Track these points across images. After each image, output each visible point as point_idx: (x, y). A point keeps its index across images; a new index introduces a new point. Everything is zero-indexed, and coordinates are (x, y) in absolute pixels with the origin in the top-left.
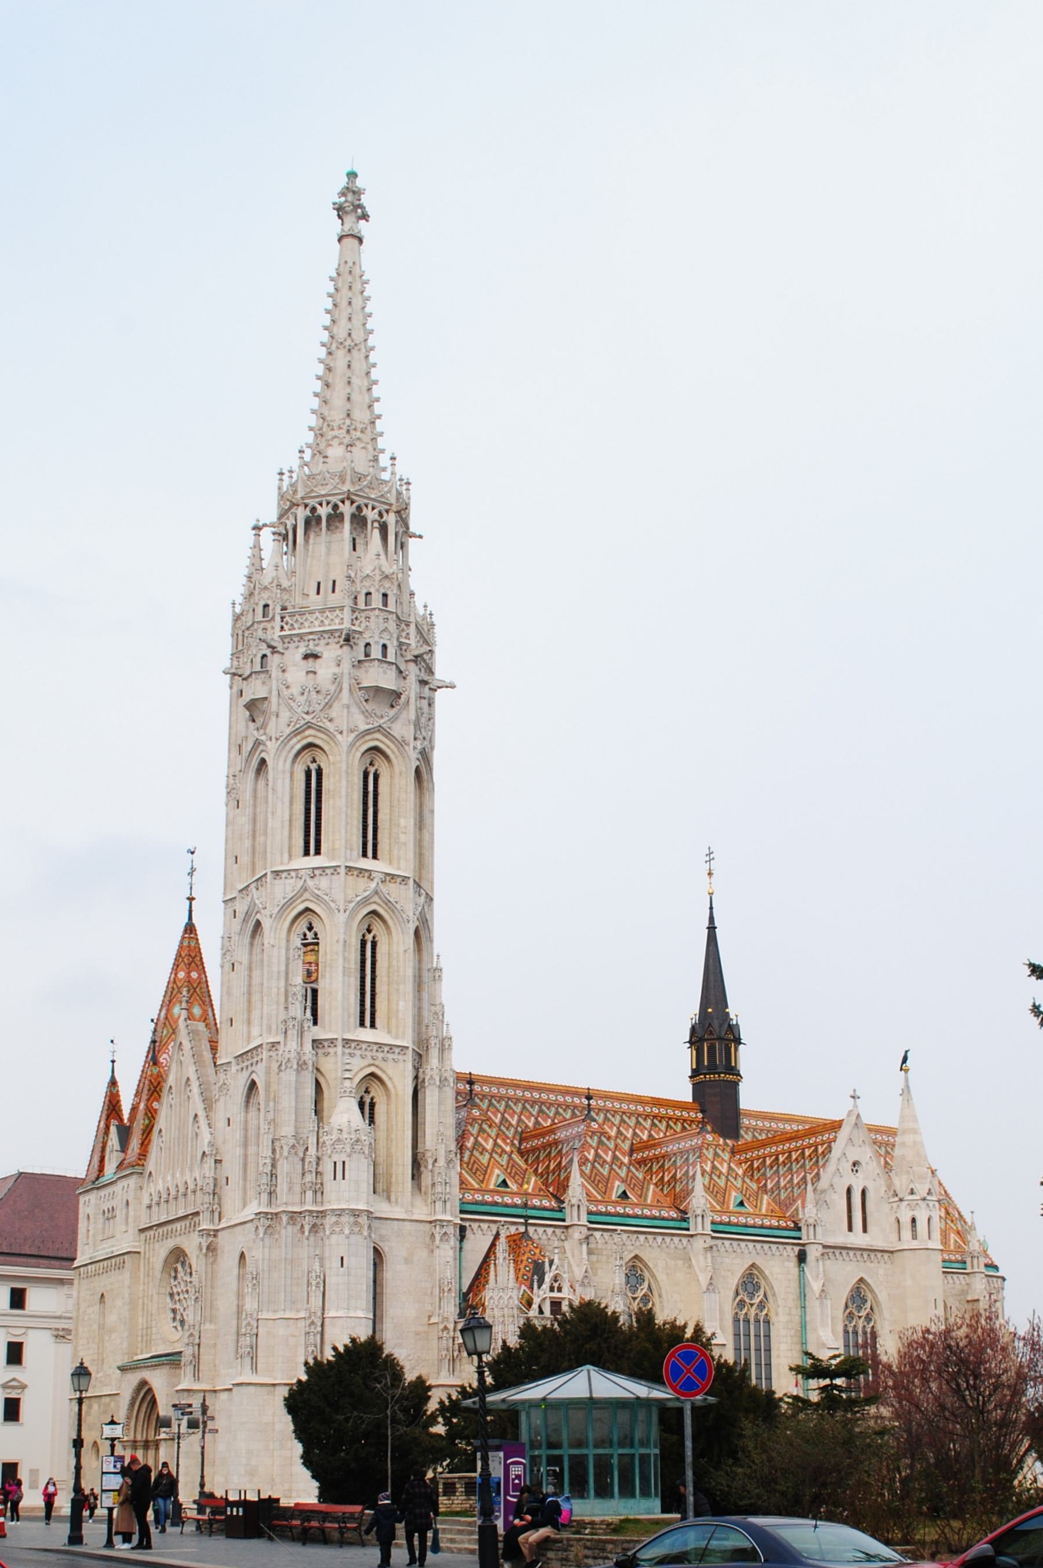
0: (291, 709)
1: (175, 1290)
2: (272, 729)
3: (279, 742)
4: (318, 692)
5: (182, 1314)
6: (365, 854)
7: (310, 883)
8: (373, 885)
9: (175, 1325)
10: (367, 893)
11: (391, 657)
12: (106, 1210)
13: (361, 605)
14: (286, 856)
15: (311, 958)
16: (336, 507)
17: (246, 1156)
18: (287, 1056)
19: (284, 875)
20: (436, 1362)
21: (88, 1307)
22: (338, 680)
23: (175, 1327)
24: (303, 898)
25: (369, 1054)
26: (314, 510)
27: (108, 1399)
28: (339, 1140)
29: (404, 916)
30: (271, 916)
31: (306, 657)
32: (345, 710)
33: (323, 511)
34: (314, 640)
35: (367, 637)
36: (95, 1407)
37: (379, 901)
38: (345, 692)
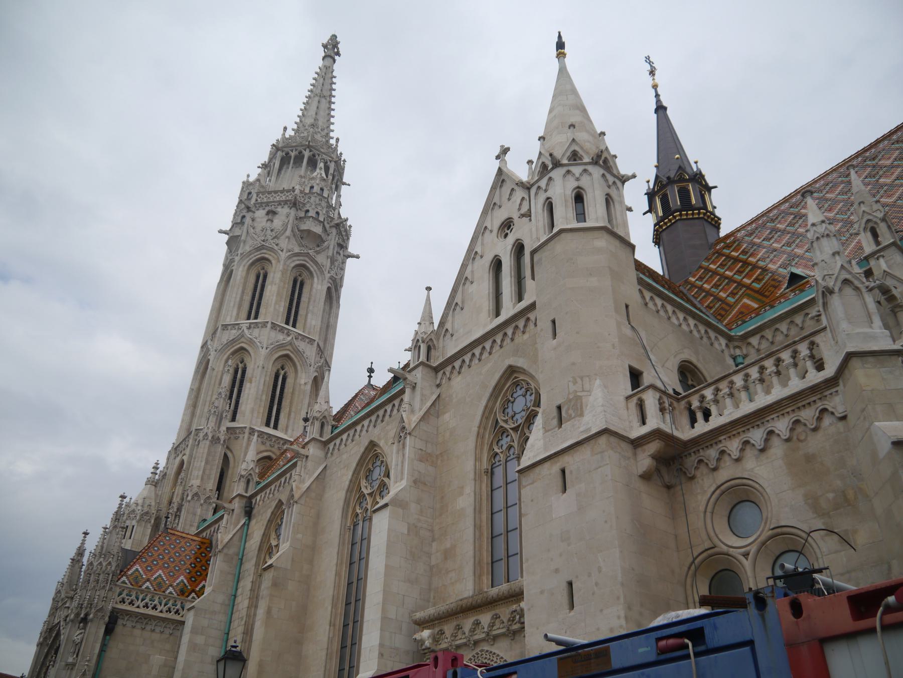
0: (253, 238)
2: (240, 252)
4: (272, 231)
6: (287, 323)
7: (246, 331)
8: (289, 338)
10: (284, 342)
11: (321, 219)
13: (307, 191)
14: (233, 319)
19: (229, 327)
24: (240, 341)
25: (268, 443)
26: (287, 154)
29: (308, 361)
32: (287, 240)
33: (293, 154)
34: (275, 205)
35: (307, 207)
37: (292, 350)
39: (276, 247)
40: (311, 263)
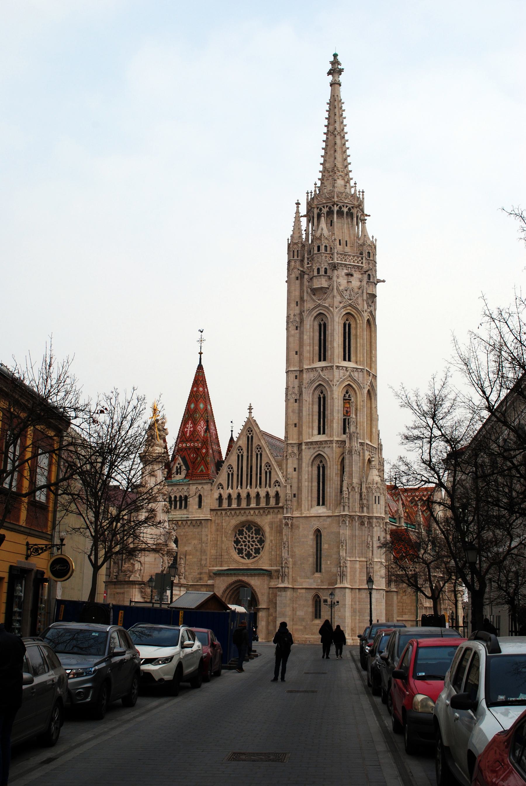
0: (342, 296)
1: (240, 539)
3: (338, 309)
5: (249, 552)
7: (352, 374)
15: (348, 406)
16: (349, 209)
17: (312, 486)
19: (341, 368)
23: (243, 557)
26: (340, 208)
33: (345, 210)
38: (365, 294)
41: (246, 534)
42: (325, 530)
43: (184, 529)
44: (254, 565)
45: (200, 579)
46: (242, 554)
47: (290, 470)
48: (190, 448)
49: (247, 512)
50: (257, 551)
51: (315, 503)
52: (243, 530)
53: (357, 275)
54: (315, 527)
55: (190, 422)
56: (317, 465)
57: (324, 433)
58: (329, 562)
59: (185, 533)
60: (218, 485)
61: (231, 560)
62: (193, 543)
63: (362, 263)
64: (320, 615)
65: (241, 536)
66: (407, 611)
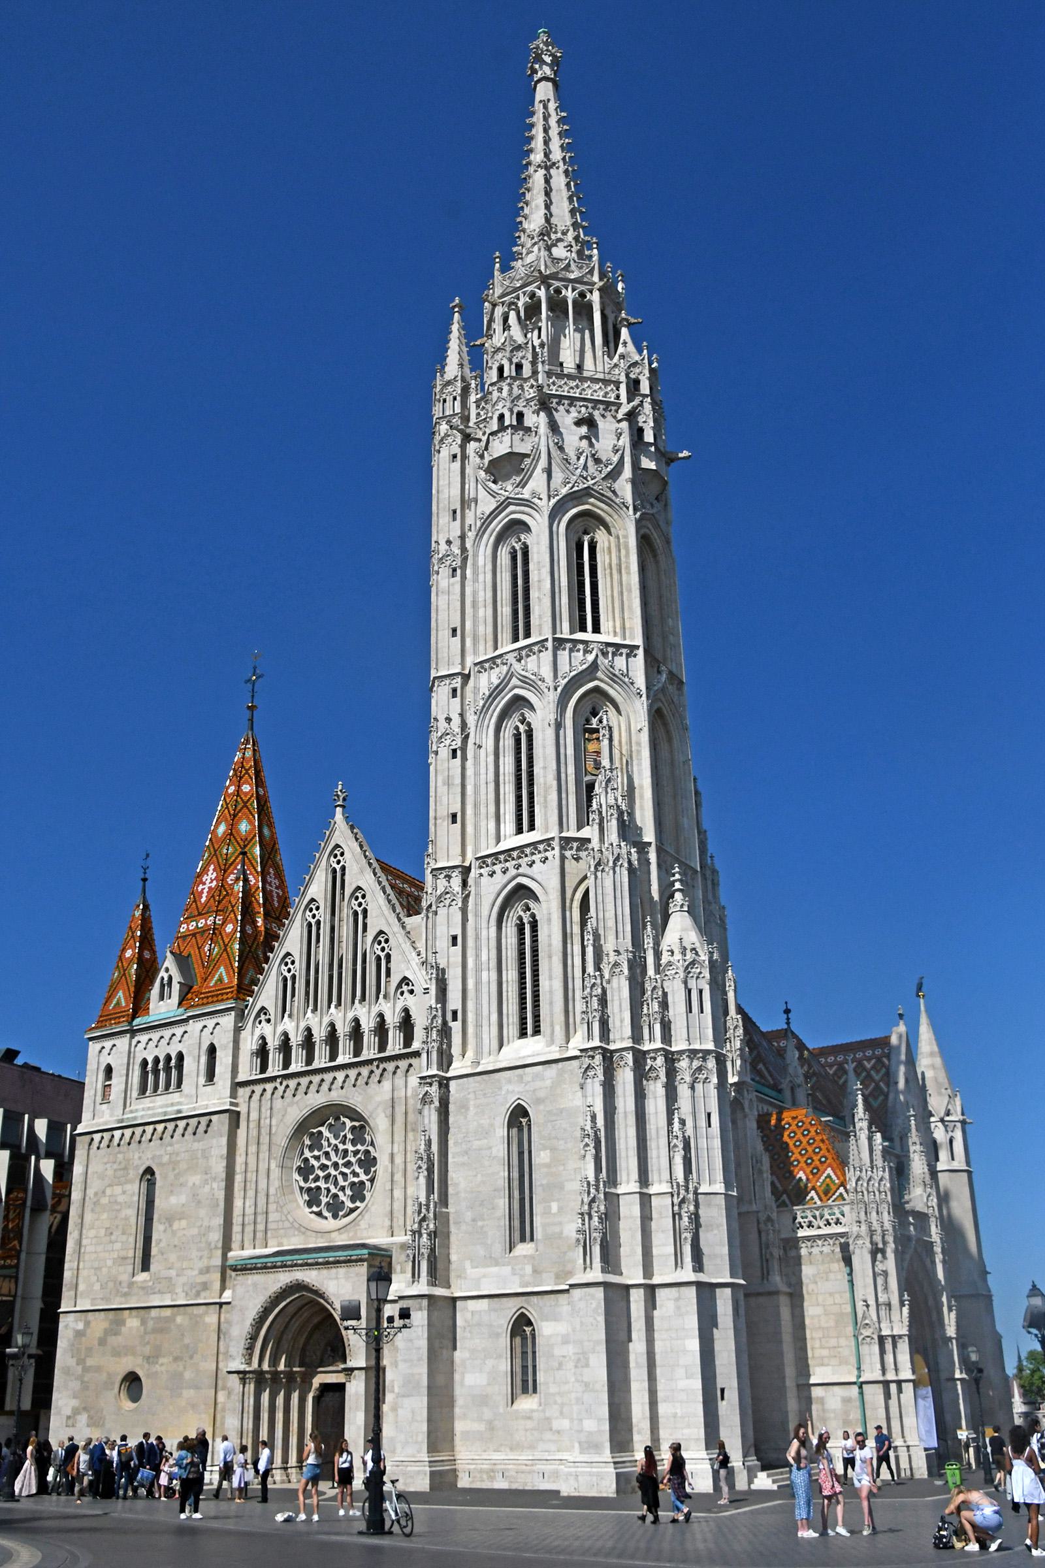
1: (313, 1162)
5: (335, 1196)
9: (315, 1209)
12: (150, 1060)
16: (582, 295)
18: (617, 851)
19: (568, 645)
20: (758, 1264)
21: (110, 1185)
22: (620, 452)
23: (319, 1214)
27: (168, 1312)
28: (693, 963)
30: (556, 690)
31: (578, 423)
36: (132, 1322)
39: (617, 500)
40: (653, 531)
41: (329, 1146)
42: (541, 1107)
43: (171, 1145)
44: (344, 1236)
45: (205, 1286)
46: (319, 1205)
47: (443, 943)
48: (204, 931)
49: (328, 1077)
50: (358, 1192)
51: (512, 1028)
52: (320, 1133)
53: (606, 425)
54: (510, 1102)
55: (212, 867)
56: (515, 921)
57: (532, 827)
58: (554, 1207)
59: (174, 1158)
60: (258, 1015)
61: (287, 1224)
62: (190, 1184)
63: (618, 397)
64: (535, 1381)
65: (316, 1153)
66: (825, 1352)
